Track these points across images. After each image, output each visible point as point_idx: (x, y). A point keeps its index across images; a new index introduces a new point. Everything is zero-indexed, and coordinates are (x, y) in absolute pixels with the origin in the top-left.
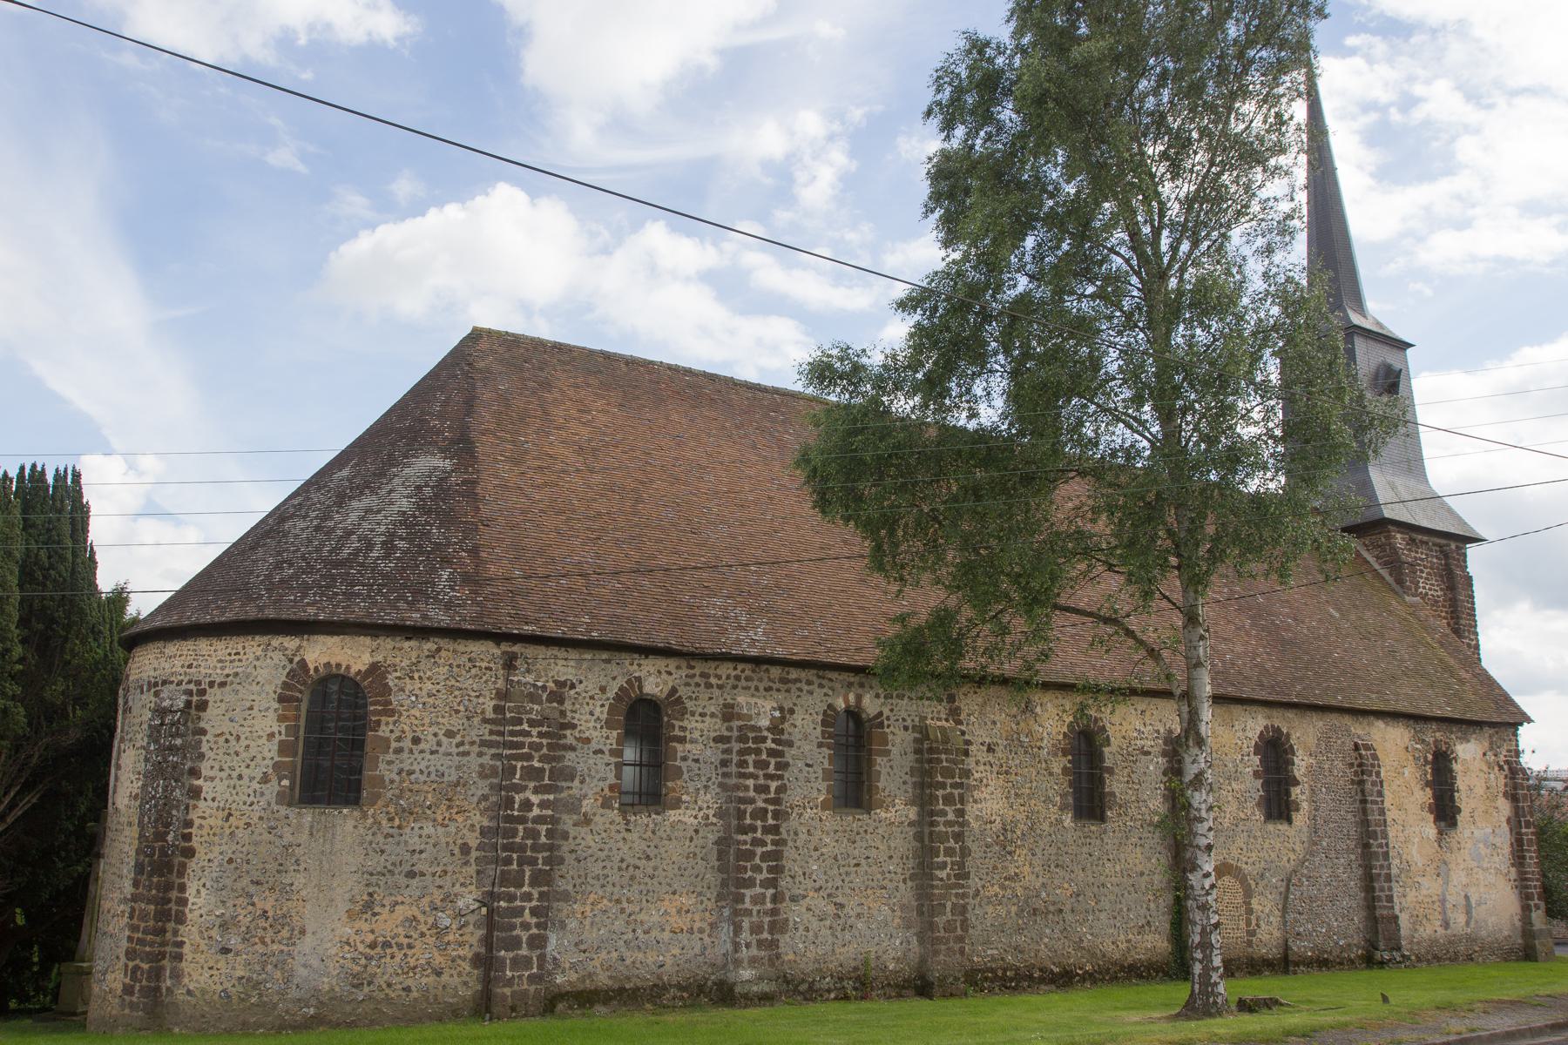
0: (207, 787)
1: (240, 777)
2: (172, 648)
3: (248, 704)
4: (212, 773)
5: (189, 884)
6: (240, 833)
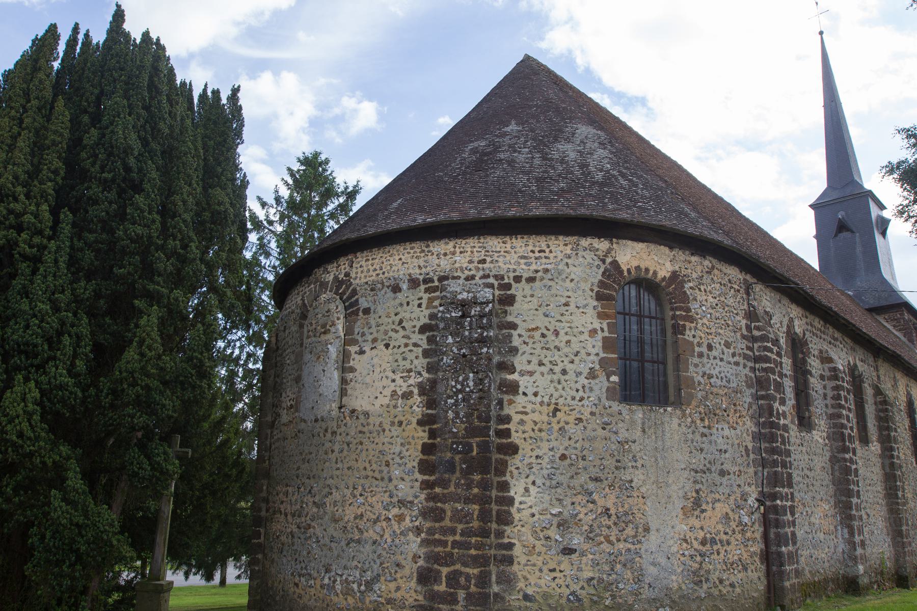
0: (524, 383)
1: (564, 372)
2: (440, 247)
3: (563, 301)
4: (533, 367)
5: (512, 482)
6: (571, 429)
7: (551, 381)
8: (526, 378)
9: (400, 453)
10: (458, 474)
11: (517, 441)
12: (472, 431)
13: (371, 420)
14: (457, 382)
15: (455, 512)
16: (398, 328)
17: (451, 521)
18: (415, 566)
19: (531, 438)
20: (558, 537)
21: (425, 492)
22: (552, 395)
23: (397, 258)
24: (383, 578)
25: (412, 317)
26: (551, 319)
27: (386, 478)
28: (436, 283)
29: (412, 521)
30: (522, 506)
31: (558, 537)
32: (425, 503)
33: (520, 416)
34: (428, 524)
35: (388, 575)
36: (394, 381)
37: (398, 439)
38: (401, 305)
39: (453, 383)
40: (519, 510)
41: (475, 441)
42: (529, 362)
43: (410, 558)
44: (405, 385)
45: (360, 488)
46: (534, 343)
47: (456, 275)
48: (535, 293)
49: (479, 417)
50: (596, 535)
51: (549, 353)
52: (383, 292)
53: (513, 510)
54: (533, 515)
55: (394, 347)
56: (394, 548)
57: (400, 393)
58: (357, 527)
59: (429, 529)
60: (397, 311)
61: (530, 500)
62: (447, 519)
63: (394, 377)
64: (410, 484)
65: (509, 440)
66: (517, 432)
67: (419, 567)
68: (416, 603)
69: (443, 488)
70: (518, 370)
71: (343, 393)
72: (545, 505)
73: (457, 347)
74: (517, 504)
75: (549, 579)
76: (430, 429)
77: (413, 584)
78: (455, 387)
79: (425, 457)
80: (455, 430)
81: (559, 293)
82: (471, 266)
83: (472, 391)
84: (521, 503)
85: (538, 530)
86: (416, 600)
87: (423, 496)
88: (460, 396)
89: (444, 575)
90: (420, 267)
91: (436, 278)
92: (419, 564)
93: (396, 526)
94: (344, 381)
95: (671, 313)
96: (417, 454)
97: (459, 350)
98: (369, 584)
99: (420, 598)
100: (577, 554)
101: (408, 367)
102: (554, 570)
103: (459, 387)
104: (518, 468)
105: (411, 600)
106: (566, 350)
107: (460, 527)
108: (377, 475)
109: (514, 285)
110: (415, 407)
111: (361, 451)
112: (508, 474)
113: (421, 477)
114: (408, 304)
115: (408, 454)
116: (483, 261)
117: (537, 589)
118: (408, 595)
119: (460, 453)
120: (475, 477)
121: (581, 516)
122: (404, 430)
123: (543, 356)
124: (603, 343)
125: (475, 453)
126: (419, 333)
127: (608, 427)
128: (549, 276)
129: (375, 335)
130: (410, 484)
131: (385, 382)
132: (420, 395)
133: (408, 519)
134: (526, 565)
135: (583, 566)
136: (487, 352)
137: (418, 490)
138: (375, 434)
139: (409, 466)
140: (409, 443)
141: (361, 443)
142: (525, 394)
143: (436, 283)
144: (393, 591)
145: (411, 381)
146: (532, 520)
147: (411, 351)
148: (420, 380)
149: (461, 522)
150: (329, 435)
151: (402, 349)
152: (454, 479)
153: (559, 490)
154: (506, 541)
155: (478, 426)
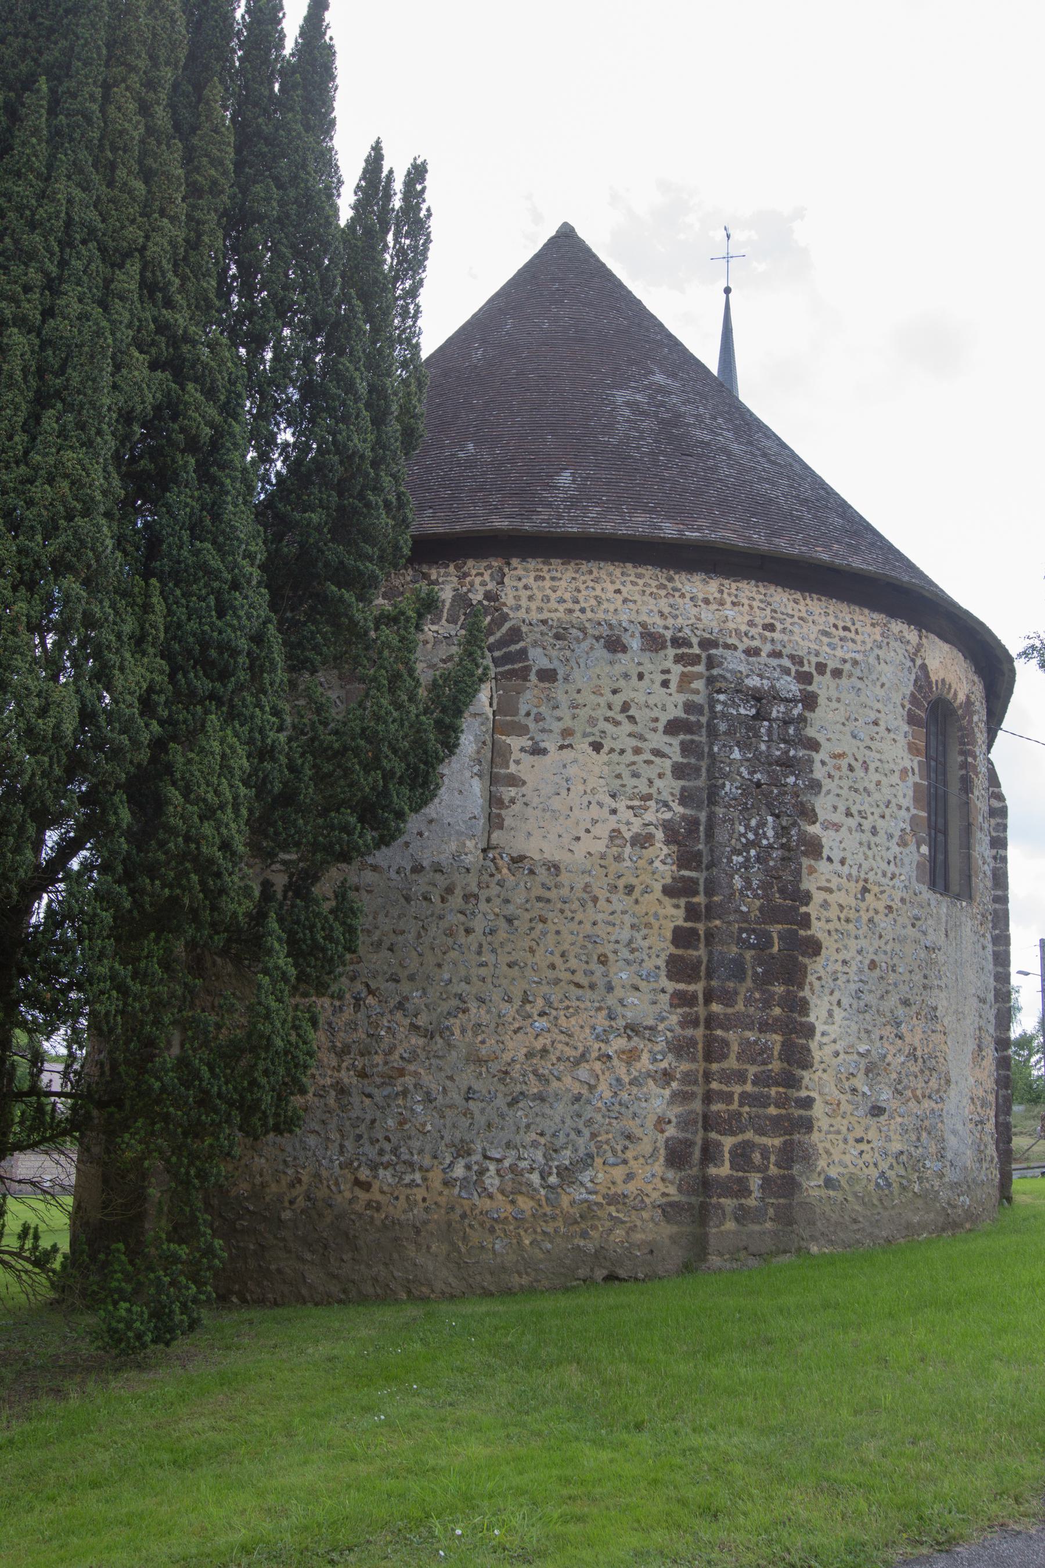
0: (829, 840)
1: (874, 832)
2: (697, 586)
3: (873, 716)
4: (838, 817)
5: (813, 1000)
6: (883, 922)
7: (861, 844)
8: (831, 833)
9: (630, 942)
10: (749, 983)
11: (821, 935)
12: (770, 914)
13: (564, 878)
14: (747, 827)
15: (745, 1044)
16: (620, 717)
17: (738, 1059)
18: (661, 1139)
19: (837, 930)
20: (866, 1089)
21: (679, 1011)
22: (860, 866)
23: (611, 588)
24: (598, 1161)
25: (651, 702)
26: (859, 743)
27: (601, 983)
28: (696, 650)
29: (655, 1060)
30: (825, 1040)
31: (866, 1089)
32: (678, 1030)
33: (823, 895)
34: (685, 1066)
35: (609, 1154)
36: (614, 812)
37: (626, 917)
38: (626, 676)
39: (742, 829)
40: (821, 1046)
41: (775, 930)
42: (835, 808)
43: (650, 1123)
44: (637, 822)
45: (540, 1002)
46: (840, 778)
47: (730, 641)
48: (842, 696)
49: (782, 891)
50: (905, 1088)
51: (858, 798)
52: (585, 645)
53: (813, 1045)
54: (837, 1054)
55: (612, 750)
56: (617, 1107)
57: (628, 835)
58: (535, 1072)
59: (686, 1074)
60: (616, 686)
61: (834, 1030)
62: (733, 1056)
63: (614, 805)
64: (651, 996)
65: (809, 933)
66: (819, 919)
67: (668, 1140)
68: (664, 1200)
69: (727, 1005)
70: (821, 818)
71: (494, 822)
72: (852, 1039)
73: (747, 768)
74: (818, 1036)
75: (856, 1153)
76: (687, 903)
77: (659, 1167)
78: (744, 835)
79: (679, 952)
80: (744, 909)
81: (869, 703)
82: (753, 631)
83: (771, 846)
84: (823, 1034)
85: (843, 1077)
86: (664, 1195)
87: (674, 1019)
88: (753, 852)
89: (726, 1149)
90: (661, 614)
91: (695, 641)
92: (667, 1134)
93: (621, 1070)
94: (494, 801)
95: (960, 758)
96: (663, 945)
97: (752, 773)
98: (567, 1174)
99: (672, 1190)
100: (886, 1116)
101: (645, 790)
102: (859, 1141)
103: (751, 836)
104: (819, 978)
105: (655, 1195)
106: (877, 796)
107: (752, 1070)
108: (579, 978)
109: (817, 678)
110: (657, 864)
111: (544, 934)
112: (807, 987)
113: (671, 986)
114: (641, 676)
115: (645, 944)
116: (770, 627)
117: (841, 1170)
118: (650, 1187)
119: (752, 947)
120: (776, 989)
121: (889, 1058)
122: (637, 902)
123: (851, 801)
124: (915, 792)
125: (776, 949)
126: (665, 732)
127: (918, 923)
128: (857, 672)
129: (568, 722)
130: (651, 996)
131: (595, 812)
132: (667, 842)
133: (645, 1057)
134: (828, 1132)
135: (891, 1134)
136: (795, 784)
137: (667, 1007)
138: (576, 905)
139: (649, 965)
140: (648, 926)
141: (543, 920)
142: (829, 859)
143: (696, 650)
144: (619, 1181)
145: (650, 816)
146: (835, 1061)
147: (648, 762)
148: (668, 816)
149: (754, 1062)
150: (456, 901)
151: (629, 757)
152: (742, 990)
153: (867, 1016)
154: (803, 1094)
155: (780, 905)
